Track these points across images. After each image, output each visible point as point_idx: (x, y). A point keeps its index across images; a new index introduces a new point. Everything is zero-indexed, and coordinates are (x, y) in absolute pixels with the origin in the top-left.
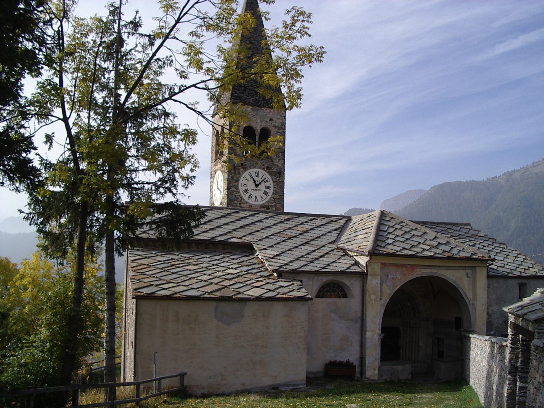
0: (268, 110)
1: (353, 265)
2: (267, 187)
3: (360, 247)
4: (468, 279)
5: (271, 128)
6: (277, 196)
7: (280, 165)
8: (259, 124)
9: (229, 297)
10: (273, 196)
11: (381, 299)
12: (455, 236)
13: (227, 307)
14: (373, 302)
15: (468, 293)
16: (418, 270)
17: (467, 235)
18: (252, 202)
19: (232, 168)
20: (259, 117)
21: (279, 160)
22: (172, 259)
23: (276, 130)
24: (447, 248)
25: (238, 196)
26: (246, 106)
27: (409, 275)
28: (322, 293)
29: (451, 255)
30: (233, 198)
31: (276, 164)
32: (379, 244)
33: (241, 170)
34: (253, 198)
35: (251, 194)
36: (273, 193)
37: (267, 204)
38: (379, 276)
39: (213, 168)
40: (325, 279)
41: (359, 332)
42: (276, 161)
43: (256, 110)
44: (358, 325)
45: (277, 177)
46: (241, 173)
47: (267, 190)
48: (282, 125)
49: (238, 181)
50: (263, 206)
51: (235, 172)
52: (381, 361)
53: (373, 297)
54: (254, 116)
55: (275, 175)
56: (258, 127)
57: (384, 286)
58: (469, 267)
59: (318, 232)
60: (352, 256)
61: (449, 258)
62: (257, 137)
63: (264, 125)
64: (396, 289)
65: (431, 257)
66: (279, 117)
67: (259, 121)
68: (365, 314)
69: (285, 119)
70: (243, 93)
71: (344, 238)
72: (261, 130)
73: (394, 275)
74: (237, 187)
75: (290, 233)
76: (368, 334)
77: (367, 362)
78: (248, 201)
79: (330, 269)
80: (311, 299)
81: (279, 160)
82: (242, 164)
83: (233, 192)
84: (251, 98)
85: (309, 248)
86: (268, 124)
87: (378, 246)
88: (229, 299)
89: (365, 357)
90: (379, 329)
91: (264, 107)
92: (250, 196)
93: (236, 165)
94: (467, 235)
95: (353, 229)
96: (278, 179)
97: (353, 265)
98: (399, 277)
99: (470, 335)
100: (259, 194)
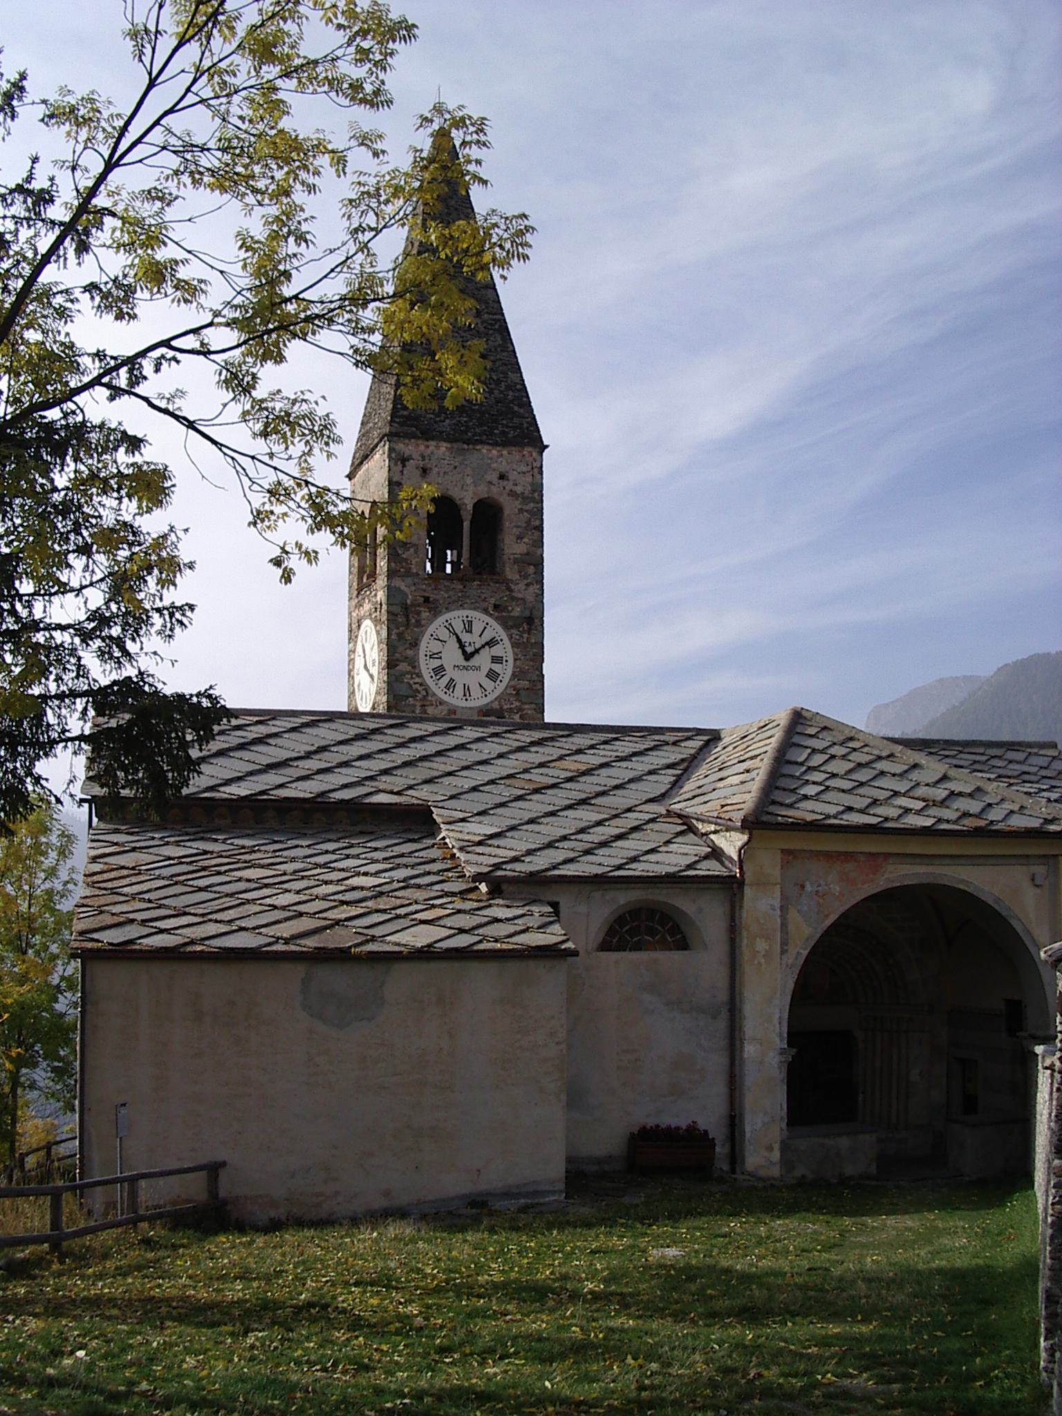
0: (494, 452)
1: (706, 857)
2: (497, 660)
3: (726, 808)
4: (1038, 891)
5: (504, 500)
7: (530, 598)
8: (471, 488)
9: (341, 950)
10: (512, 683)
11: (783, 952)
12: (1009, 777)
13: (334, 978)
14: (763, 961)
16: (891, 868)
17: (1044, 773)
18: (456, 699)
19: (396, 609)
20: (469, 471)
21: (527, 585)
22: (205, 852)
23: (517, 504)
24: (974, 806)
25: (417, 686)
26: (433, 443)
27: (864, 883)
29: (982, 823)
30: (403, 690)
31: (520, 596)
32: (779, 799)
33: (425, 615)
34: (459, 691)
35: (452, 680)
36: (514, 675)
37: (496, 705)
38: (777, 890)
39: (354, 614)
40: (624, 898)
42: (519, 589)
43: (461, 451)
44: (722, 1024)
45: (524, 631)
46: (423, 622)
47: (496, 667)
48: (534, 491)
49: (415, 644)
50: (486, 711)
51: (408, 620)
52: (788, 1125)
53: (761, 945)
54: (455, 468)
55: (517, 627)
56: (467, 500)
57: (793, 915)
58: (1039, 856)
59: (621, 773)
60: (706, 834)
61: (978, 832)
62: (466, 525)
63: (483, 491)
64: (828, 922)
66: (524, 469)
67: (469, 481)
68: (741, 994)
69: (541, 473)
71: (689, 786)
72: (475, 505)
73: (823, 883)
74: (413, 663)
75: (538, 777)
76: (750, 1050)
77: (748, 1129)
78: (445, 698)
79: (638, 869)
80: (574, 953)
81: (527, 585)
82: (427, 600)
83: (403, 674)
84: (447, 421)
85: (587, 815)
86: (494, 489)
87: (774, 802)
88: (341, 956)
89: (742, 1116)
90: (780, 1035)
91: (482, 442)
92: (451, 685)
93: (409, 602)
94: (1044, 773)
95: (718, 763)
96: (525, 635)
97: (706, 857)
100: (474, 679)
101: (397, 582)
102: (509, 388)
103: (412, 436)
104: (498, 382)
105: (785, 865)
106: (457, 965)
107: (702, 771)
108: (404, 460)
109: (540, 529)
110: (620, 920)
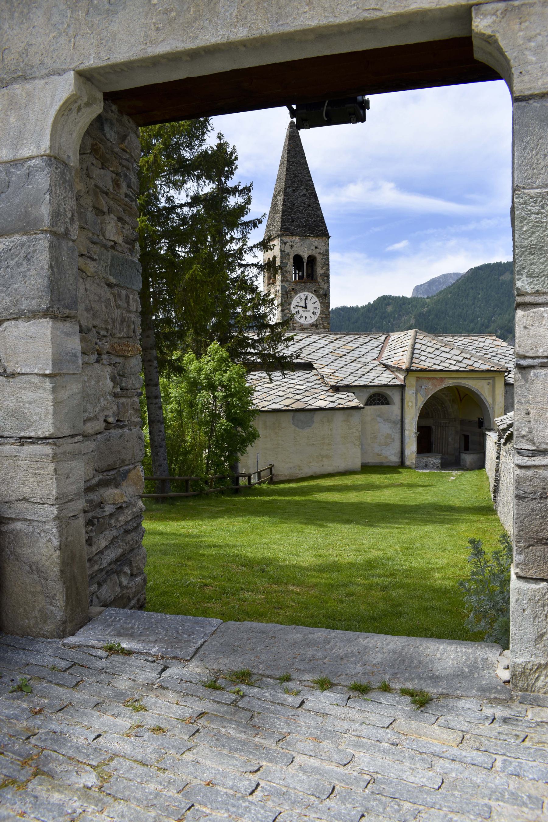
2: (315, 308)
5: (317, 255)
6: (324, 316)
7: (325, 288)
13: (301, 416)
15: (488, 399)
17: (491, 346)
18: (303, 321)
19: (284, 293)
24: (470, 362)
28: (371, 401)
29: (473, 368)
33: (293, 294)
34: (304, 319)
36: (321, 313)
40: (372, 391)
41: (399, 431)
42: (322, 285)
43: (303, 240)
44: (399, 426)
47: (315, 311)
50: (312, 325)
53: (410, 404)
55: (321, 297)
56: (305, 255)
57: (419, 395)
59: (363, 350)
61: (472, 371)
62: (305, 264)
63: (310, 253)
65: (457, 371)
70: (290, 224)
71: (385, 355)
75: (340, 352)
76: (407, 433)
77: (406, 454)
79: (376, 382)
80: (363, 408)
82: (293, 289)
85: (356, 365)
86: (314, 252)
88: (303, 410)
94: (491, 346)
95: (392, 346)
98: (431, 387)
99: (487, 432)
100: (308, 314)
101: (284, 284)
102: (318, 216)
103: (287, 235)
104: (314, 215)
105: (417, 381)
106: (332, 411)
107: (387, 349)
108: (285, 243)
109: (328, 265)
110: (371, 397)
